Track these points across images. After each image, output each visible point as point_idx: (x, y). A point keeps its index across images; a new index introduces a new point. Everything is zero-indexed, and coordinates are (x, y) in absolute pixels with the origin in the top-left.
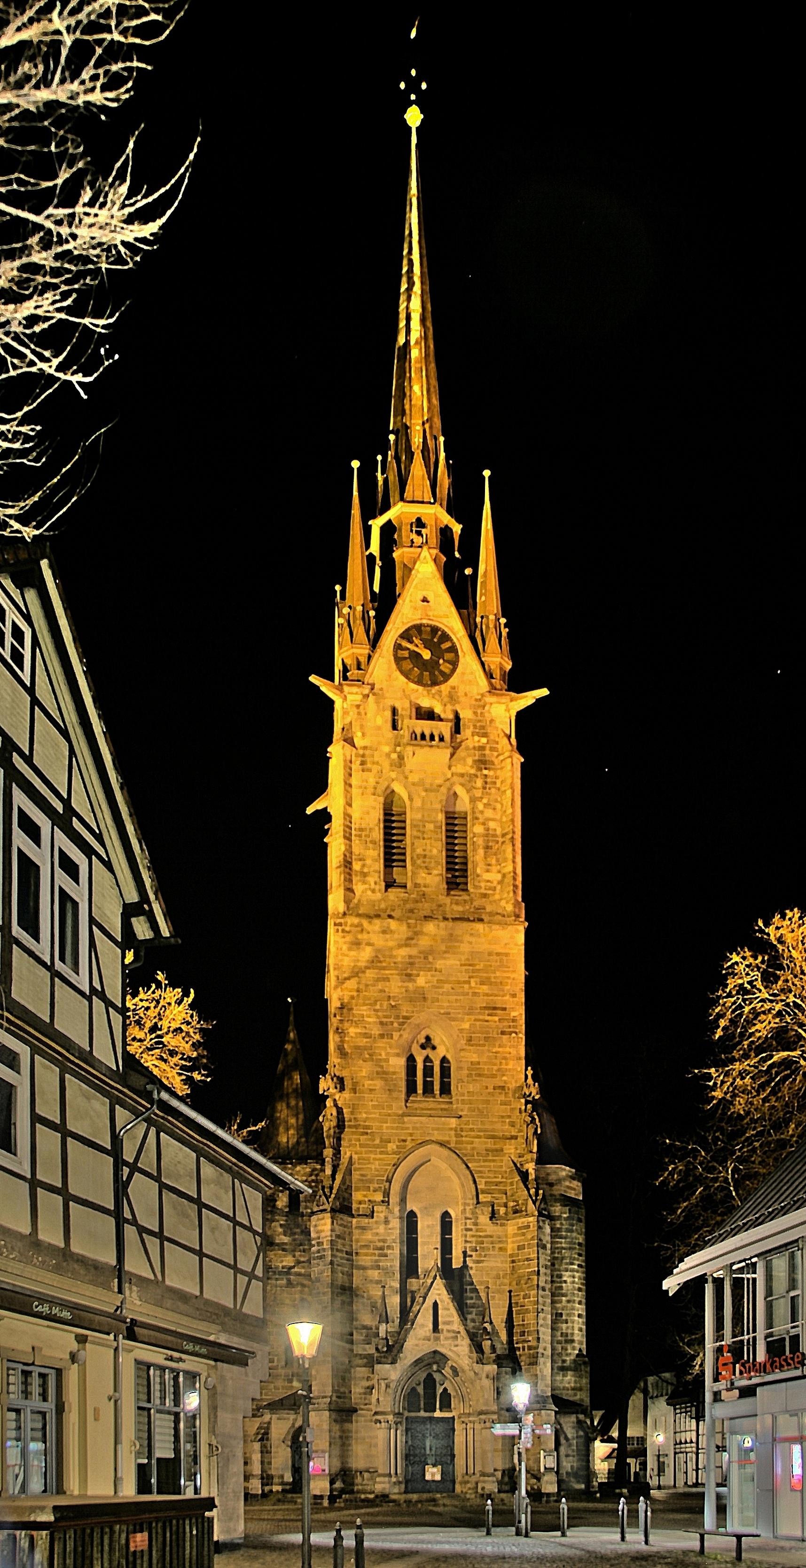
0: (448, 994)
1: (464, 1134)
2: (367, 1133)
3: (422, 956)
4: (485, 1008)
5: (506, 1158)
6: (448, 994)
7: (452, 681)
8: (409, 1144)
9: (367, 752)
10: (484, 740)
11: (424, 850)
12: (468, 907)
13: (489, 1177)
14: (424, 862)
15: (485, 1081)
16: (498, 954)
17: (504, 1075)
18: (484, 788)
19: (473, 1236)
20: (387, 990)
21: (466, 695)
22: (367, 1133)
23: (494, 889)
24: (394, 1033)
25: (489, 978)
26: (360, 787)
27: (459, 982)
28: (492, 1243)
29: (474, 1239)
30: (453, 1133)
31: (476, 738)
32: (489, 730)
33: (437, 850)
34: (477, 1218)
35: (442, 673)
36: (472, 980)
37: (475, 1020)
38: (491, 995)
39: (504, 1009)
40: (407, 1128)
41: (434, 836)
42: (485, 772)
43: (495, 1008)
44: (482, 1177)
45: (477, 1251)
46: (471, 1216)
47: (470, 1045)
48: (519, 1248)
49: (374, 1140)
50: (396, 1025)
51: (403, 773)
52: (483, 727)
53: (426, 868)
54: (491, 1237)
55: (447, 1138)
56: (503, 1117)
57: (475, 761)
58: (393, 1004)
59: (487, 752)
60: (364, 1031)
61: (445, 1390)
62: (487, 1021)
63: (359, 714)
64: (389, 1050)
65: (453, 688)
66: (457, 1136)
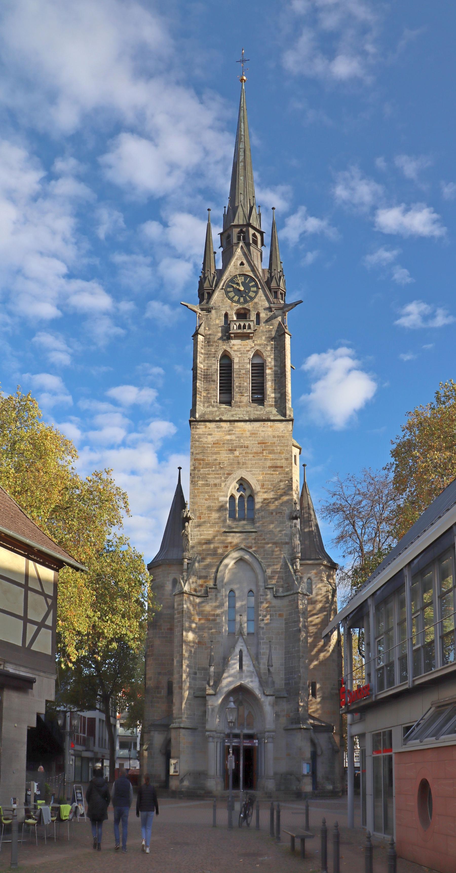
0: (251, 460)
1: (259, 542)
3: (237, 439)
6: (251, 460)
7: (256, 300)
10: (271, 327)
11: (240, 384)
12: (262, 412)
14: (240, 390)
16: (278, 437)
21: (262, 306)
24: (222, 484)
25: (274, 450)
27: (256, 453)
28: (275, 611)
31: (267, 327)
35: (250, 297)
37: (266, 474)
38: (275, 460)
39: (282, 467)
41: (245, 376)
47: (263, 488)
50: (223, 478)
51: (230, 345)
53: (241, 393)
57: (266, 338)
58: (222, 466)
60: (206, 483)
61: (250, 712)
62: (272, 474)
63: (207, 319)
65: (256, 303)
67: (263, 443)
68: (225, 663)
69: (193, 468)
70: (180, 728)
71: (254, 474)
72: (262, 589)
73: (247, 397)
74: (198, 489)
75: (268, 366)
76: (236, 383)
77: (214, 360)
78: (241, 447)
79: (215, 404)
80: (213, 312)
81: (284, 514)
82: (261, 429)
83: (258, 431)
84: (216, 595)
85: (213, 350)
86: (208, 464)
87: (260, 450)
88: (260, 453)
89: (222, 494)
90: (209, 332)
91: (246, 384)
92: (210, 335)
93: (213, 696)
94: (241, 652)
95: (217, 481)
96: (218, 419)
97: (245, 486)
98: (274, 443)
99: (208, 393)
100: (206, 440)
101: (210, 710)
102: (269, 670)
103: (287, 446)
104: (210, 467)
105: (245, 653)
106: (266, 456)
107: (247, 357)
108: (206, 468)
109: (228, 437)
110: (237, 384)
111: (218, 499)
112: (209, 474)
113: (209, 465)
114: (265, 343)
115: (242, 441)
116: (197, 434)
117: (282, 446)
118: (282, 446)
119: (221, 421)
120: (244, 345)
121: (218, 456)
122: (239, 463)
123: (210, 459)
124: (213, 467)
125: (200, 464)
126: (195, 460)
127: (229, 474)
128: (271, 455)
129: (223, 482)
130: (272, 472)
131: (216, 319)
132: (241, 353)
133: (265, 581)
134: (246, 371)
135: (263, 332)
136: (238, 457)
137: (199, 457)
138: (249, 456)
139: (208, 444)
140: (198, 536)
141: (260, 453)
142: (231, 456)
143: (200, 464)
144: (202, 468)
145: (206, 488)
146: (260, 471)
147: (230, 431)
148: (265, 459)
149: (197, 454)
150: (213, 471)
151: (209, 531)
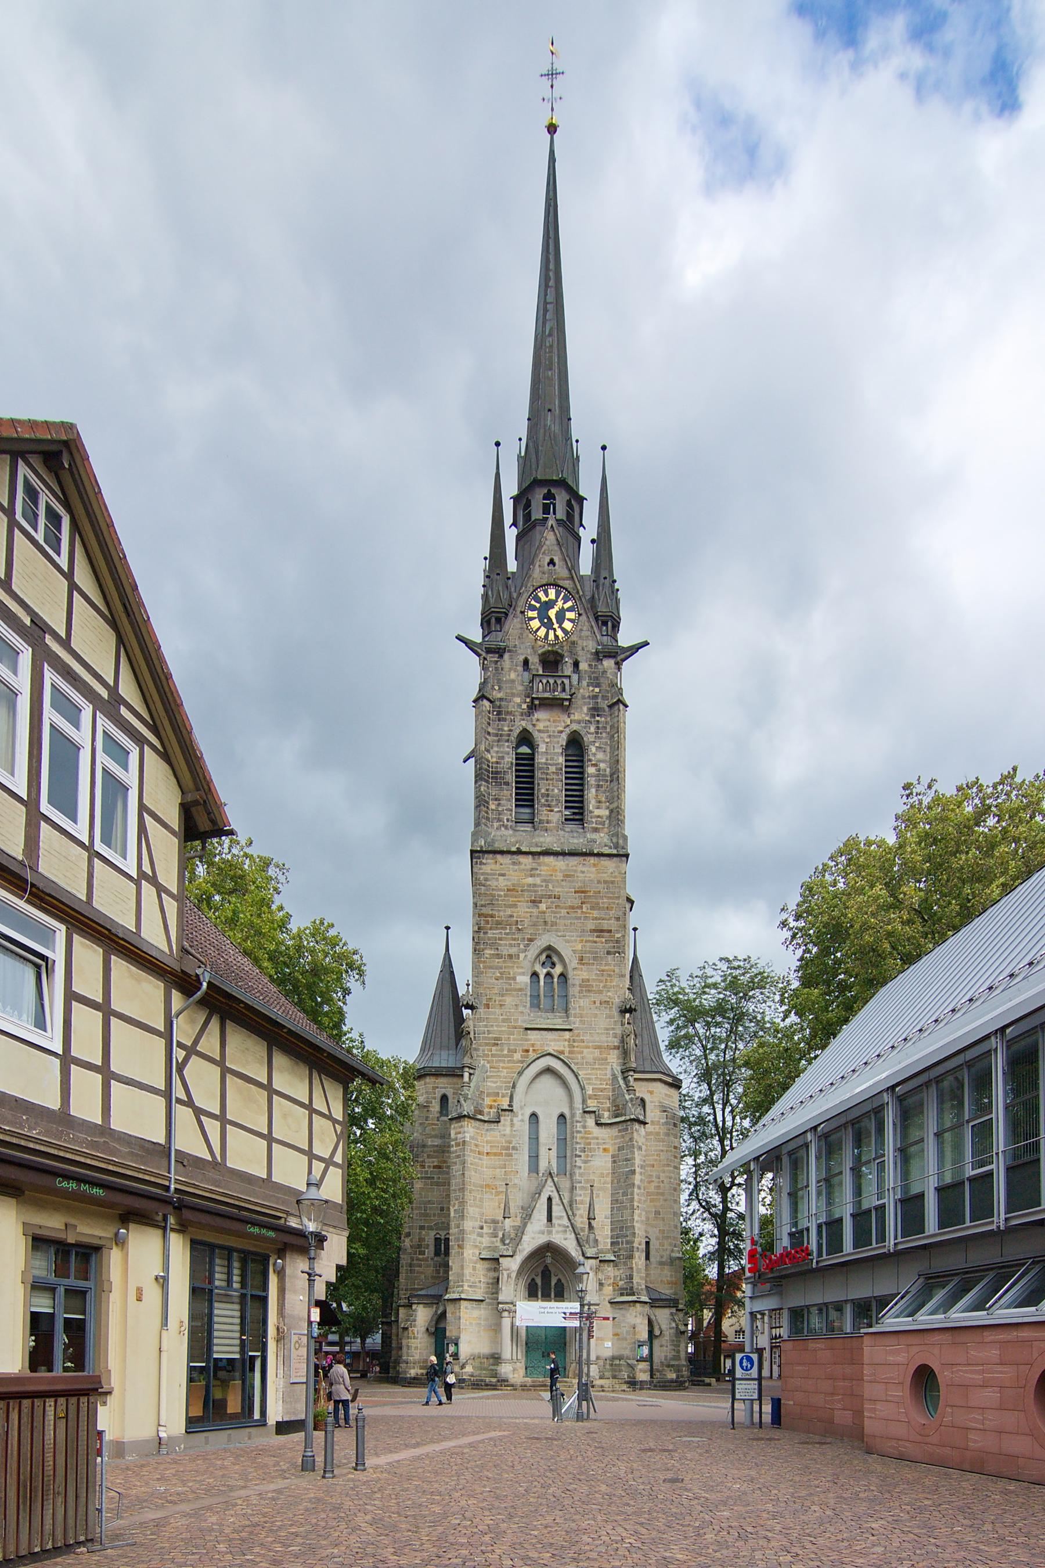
0: (564, 918)
4: (594, 931)
5: (609, 1067)
8: (532, 1055)
10: (597, 690)
11: (547, 790)
15: (594, 997)
16: (606, 882)
18: (597, 733)
19: (582, 1138)
23: (603, 824)
26: (496, 735)
27: (573, 908)
29: (583, 1141)
31: (591, 688)
32: (602, 680)
39: (610, 931)
41: (555, 777)
42: (598, 718)
43: (602, 931)
44: (589, 1084)
48: (620, 1149)
49: (502, 1050)
50: (522, 946)
52: (597, 678)
53: (549, 806)
54: (597, 1138)
55: (562, 1048)
56: (607, 1029)
57: (589, 709)
61: (559, 1280)
62: (595, 942)
63: (496, 669)
64: (516, 970)
66: (571, 1046)
67: (583, 892)
68: (527, 1215)
69: (476, 929)
70: (461, 1299)
71: (568, 941)
72: (579, 1112)
74: (484, 962)
75: (590, 760)
76: (542, 787)
77: (508, 747)
78: (550, 897)
79: (509, 824)
80: (506, 656)
82: (580, 868)
83: (575, 871)
84: (512, 1120)
85: (506, 729)
86: (498, 923)
87: (577, 902)
89: (521, 970)
90: (499, 696)
91: (556, 791)
92: (501, 699)
93: (509, 1259)
94: (550, 1199)
95: (513, 951)
96: (514, 849)
97: (555, 959)
99: (499, 805)
100: (496, 883)
101: (505, 1276)
102: (590, 1223)
104: (502, 928)
105: (556, 1200)
109: (530, 880)
110: (543, 791)
111: (514, 979)
112: (500, 939)
114: (587, 718)
115: (550, 887)
116: (482, 874)
117: (610, 898)
118: (610, 898)
119: (519, 852)
123: (502, 914)
125: (487, 922)
126: (479, 916)
127: (531, 940)
128: (595, 912)
131: (510, 669)
132: (550, 736)
133: (584, 1101)
135: (583, 697)
136: (544, 913)
137: (484, 911)
142: (534, 910)
143: (487, 922)
144: (491, 929)
147: (532, 869)
149: (482, 906)
150: (507, 934)
151: (500, 1026)
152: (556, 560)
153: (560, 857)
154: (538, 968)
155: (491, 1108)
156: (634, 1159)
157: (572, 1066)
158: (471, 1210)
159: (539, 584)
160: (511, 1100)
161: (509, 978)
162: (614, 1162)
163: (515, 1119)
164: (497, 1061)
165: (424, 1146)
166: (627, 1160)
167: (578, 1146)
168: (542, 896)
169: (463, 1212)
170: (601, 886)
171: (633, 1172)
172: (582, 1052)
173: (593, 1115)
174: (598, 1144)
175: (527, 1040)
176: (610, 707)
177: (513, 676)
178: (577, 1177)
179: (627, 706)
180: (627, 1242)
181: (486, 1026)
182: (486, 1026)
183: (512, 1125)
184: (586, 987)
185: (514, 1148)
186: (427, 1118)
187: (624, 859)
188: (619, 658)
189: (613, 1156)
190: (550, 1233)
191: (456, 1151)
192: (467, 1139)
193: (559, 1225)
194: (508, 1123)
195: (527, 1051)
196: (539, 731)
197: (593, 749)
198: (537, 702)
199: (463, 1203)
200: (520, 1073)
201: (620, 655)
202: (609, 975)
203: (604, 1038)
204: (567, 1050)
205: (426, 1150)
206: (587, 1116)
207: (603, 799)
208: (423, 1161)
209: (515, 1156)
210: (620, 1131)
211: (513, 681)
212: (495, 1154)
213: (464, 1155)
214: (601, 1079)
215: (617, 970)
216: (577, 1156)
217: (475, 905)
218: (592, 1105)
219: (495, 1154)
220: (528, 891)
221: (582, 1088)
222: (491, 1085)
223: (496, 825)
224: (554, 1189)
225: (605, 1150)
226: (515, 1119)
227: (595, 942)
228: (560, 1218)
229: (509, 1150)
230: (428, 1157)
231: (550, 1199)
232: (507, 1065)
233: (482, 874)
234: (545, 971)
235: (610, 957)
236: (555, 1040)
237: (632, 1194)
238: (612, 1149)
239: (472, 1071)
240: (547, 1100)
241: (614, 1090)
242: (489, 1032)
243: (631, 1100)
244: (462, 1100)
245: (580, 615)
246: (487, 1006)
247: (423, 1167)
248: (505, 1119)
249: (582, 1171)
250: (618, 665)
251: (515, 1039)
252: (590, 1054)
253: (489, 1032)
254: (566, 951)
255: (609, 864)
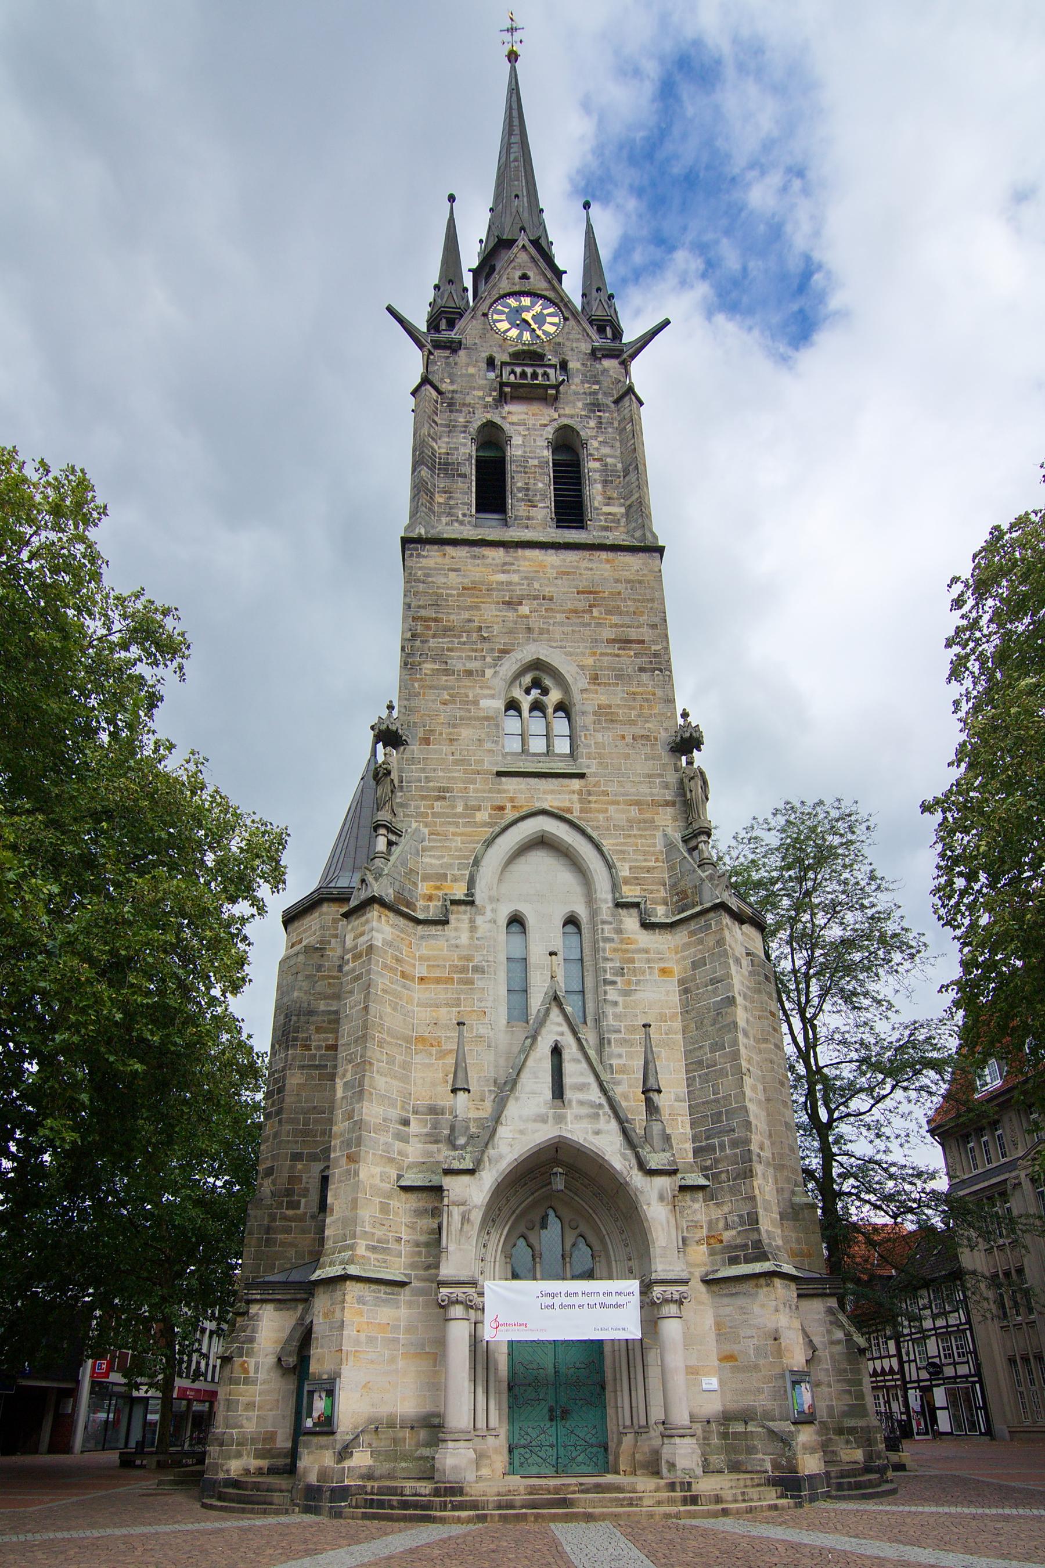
0: (562, 624)
1: (592, 798)
2: (444, 798)
3: (525, 582)
4: (614, 641)
5: (659, 834)
8: (510, 815)
9: (456, 396)
10: (597, 387)
11: (527, 484)
13: (636, 860)
14: (526, 495)
15: (620, 730)
16: (628, 581)
17: (647, 722)
19: (615, 950)
20: (476, 619)
22: (444, 798)
24: (487, 671)
25: (619, 607)
27: (575, 611)
28: (648, 961)
30: (576, 797)
31: (587, 385)
32: (602, 378)
33: (544, 485)
34: (621, 921)
36: (594, 610)
37: (602, 654)
38: (622, 626)
39: (643, 642)
40: (505, 791)
42: (598, 414)
44: (624, 860)
45: (623, 975)
46: (610, 919)
47: (595, 684)
48: (695, 965)
49: (454, 807)
50: (488, 660)
51: (500, 413)
54: (647, 951)
55: (567, 804)
56: (649, 776)
58: (486, 635)
59: (600, 396)
60: (443, 667)
62: (618, 656)
63: (448, 364)
64: (479, 691)
66: (581, 801)
67: (591, 593)
68: (506, 1087)
69: (409, 635)
72: (606, 906)
73: (544, 511)
76: (516, 481)
77: (464, 438)
78: (536, 598)
79: (467, 519)
81: (656, 739)
82: (585, 564)
83: (577, 567)
84: (472, 921)
85: (461, 420)
88: (584, 612)
89: (486, 692)
90: (451, 388)
94: (556, 1051)
97: (548, 682)
98: (619, 593)
99: (450, 498)
100: (443, 580)
103: (652, 600)
104: (455, 636)
105: (570, 1050)
106: (599, 619)
107: (542, 436)
108: (444, 636)
109: (502, 577)
110: (520, 485)
111: (476, 703)
112: (450, 650)
113: (450, 630)
114: (583, 413)
115: (536, 585)
116: (420, 568)
117: (639, 601)
120: (533, 415)
121: (474, 613)
122: (529, 630)
123: (455, 618)
124: (461, 636)
125: (429, 628)
126: (414, 619)
127: (505, 652)
128: (613, 617)
129: (490, 667)
130: (617, 652)
131: (468, 365)
132: (528, 429)
133: (615, 887)
134: (540, 462)
135: (576, 393)
136: (527, 617)
137: (423, 613)
138: (555, 617)
139: (451, 588)
140: (420, 781)
141: (584, 612)
142: (510, 614)
143: (429, 628)
144: (434, 636)
145: (445, 678)
146: (586, 647)
147: (505, 564)
148: (598, 625)
149: (419, 607)
150: (464, 643)
152: (530, 274)
153: (551, 552)
154: (518, 693)
155: (430, 898)
156: (729, 976)
157: (589, 830)
158: (380, 1082)
159: (507, 291)
160: (471, 883)
161: (467, 703)
162: (686, 991)
163: (479, 920)
164: (442, 824)
165: (311, 1013)
166: (714, 981)
167: (609, 965)
168: (523, 597)
169: (361, 1084)
170: (621, 587)
171: (731, 1001)
172: (606, 811)
173: (634, 912)
174: (648, 961)
175: (499, 792)
176: (616, 402)
177: (471, 370)
178: (610, 1021)
179: (641, 404)
180: (734, 1144)
181: (423, 770)
182: (423, 770)
183: (473, 928)
184: (605, 715)
185: (477, 969)
186: (319, 968)
187: (657, 555)
188: (625, 356)
189: (681, 982)
190: (560, 1119)
191: (354, 970)
192: (378, 943)
193: (581, 1103)
194: (466, 925)
195: (502, 808)
196: (512, 424)
197: (595, 444)
198: (507, 389)
199: (363, 1065)
200: (489, 843)
201: (625, 356)
202: (647, 700)
203: (644, 789)
204: (577, 806)
205: (315, 1018)
206: (623, 912)
207: (615, 495)
208: (309, 1038)
209: (479, 984)
210: (692, 934)
211: (472, 375)
212: (438, 981)
213: (369, 972)
214: (645, 853)
215: (659, 693)
216: (606, 982)
217: (408, 606)
218: (630, 893)
219: (438, 981)
220: (499, 590)
221: (610, 866)
222: (430, 862)
223: (444, 520)
224: (565, 1028)
225: (664, 971)
226: (479, 920)
227: (618, 656)
228: (582, 1087)
229: (467, 972)
230: (319, 1030)
231: (556, 1051)
232: (461, 830)
233: (420, 568)
234: (530, 698)
235: (645, 676)
236: (552, 792)
237: (735, 1042)
238: (677, 969)
239: (393, 838)
240: (546, 891)
241: (671, 868)
242: (428, 779)
243: (711, 878)
244: (370, 878)
245: (566, 319)
246: (426, 741)
247: (308, 1047)
248: (460, 918)
249: (619, 1009)
250: (625, 364)
251: (478, 789)
252: (618, 814)
253: (428, 779)
254: (567, 668)
255: (634, 562)
